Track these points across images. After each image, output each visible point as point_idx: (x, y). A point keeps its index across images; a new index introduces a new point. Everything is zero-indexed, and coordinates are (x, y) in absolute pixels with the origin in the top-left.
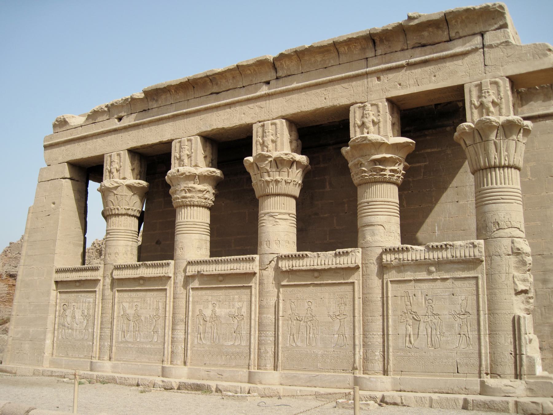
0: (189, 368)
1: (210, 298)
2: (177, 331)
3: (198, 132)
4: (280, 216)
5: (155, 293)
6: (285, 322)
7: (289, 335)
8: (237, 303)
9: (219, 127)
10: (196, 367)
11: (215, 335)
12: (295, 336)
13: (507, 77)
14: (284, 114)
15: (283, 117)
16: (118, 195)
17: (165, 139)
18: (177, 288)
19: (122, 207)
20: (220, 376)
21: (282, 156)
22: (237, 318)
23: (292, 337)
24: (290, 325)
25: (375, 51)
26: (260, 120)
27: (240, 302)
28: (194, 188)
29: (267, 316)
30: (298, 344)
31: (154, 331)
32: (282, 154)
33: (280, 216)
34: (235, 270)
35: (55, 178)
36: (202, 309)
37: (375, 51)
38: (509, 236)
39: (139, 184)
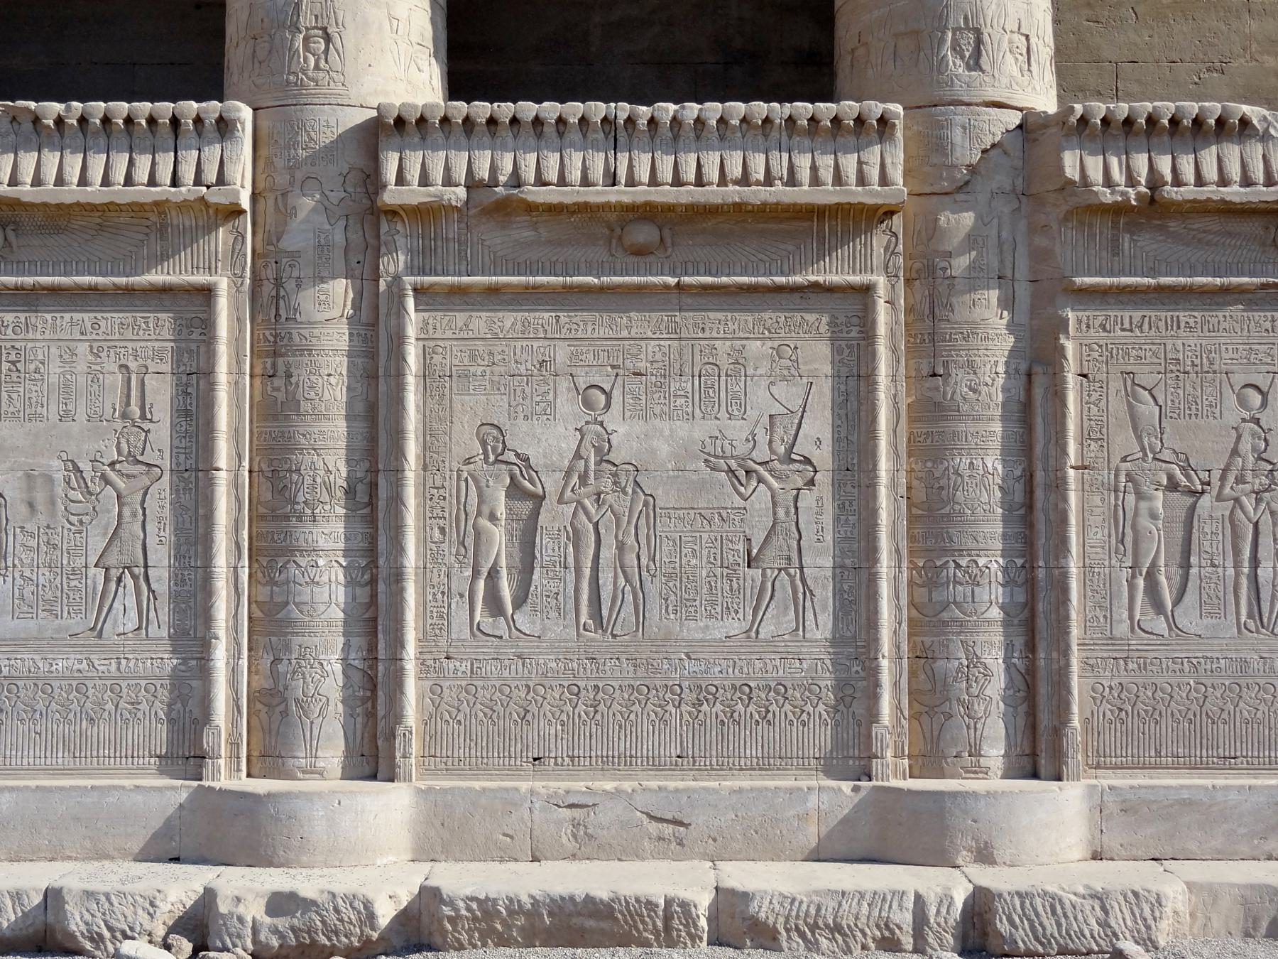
0: (419, 790)
1: (562, 354)
2: (303, 561)
5: (111, 321)
6: (1097, 500)
7: (1125, 574)
8: (764, 383)
10: (477, 785)
11: (606, 578)
12: (1163, 579)
18: (290, 285)
20: (668, 829)
22: (766, 475)
23: (1141, 582)
24: (1130, 515)
27: (784, 378)
29: (976, 462)
30: (1182, 622)
31: (112, 559)
34: (758, 183)
36: (501, 419)
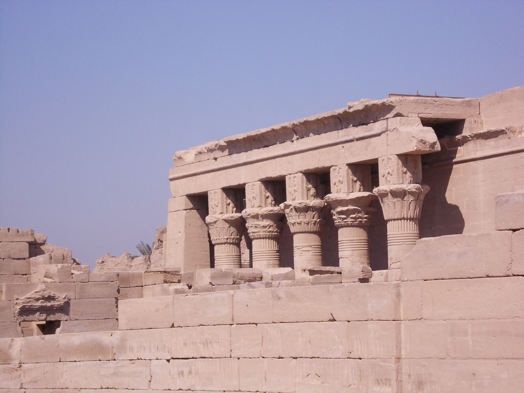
3: (259, 178)
4: (303, 249)
9: (269, 176)
13: (396, 155)
14: (300, 170)
15: (301, 172)
16: (217, 228)
17: (241, 183)
19: (222, 237)
21: (297, 205)
25: (342, 125)
26: (289, 173)
28: (259, 225)
32: (296, 204)
33: (303, 249)
35: (179, 210)
37: (342, 125)
38: (398, 268)
39: (232, 217)
